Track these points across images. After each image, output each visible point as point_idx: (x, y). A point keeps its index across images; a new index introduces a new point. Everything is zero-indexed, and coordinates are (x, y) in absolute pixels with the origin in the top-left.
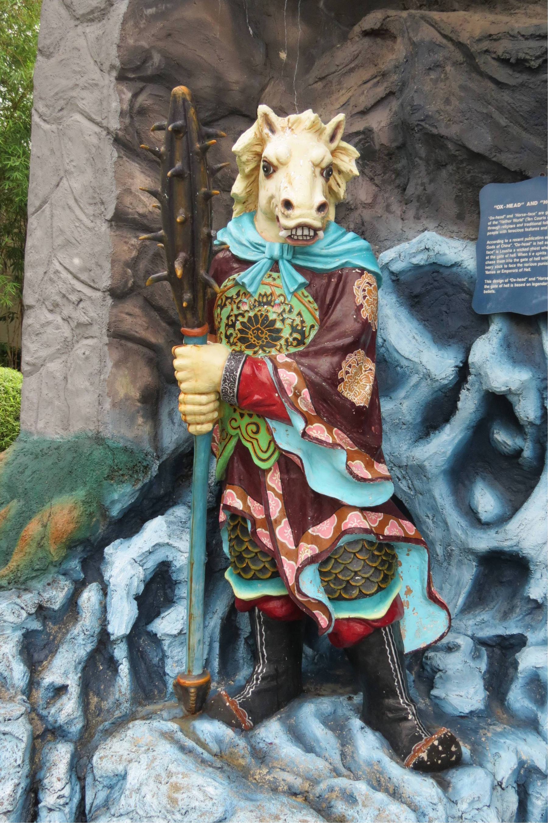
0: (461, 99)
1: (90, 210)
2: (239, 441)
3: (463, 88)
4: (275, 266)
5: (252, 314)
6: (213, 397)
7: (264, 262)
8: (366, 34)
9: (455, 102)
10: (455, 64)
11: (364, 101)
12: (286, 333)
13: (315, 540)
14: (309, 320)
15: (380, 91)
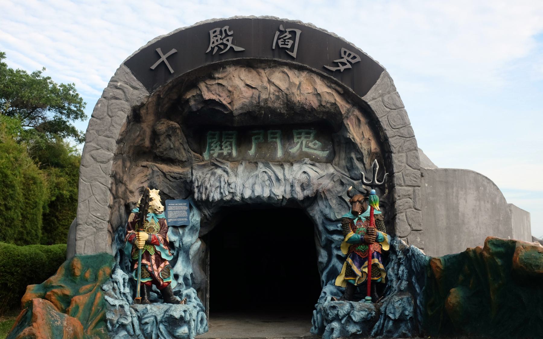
0: (162, 182)
1: (103, 204)
2: (146, 250)
3: (163, 180)
4: (153, 217)
5: (149, 226)
6: (145, 242)
7: (151, 217)
8: (142, 166)
9: (161, 183)
10: (161, 175)
11: (143, 181)
12: (156, 230)
13: (161, 267)
14: (159, 228)
15: (146, 179)
